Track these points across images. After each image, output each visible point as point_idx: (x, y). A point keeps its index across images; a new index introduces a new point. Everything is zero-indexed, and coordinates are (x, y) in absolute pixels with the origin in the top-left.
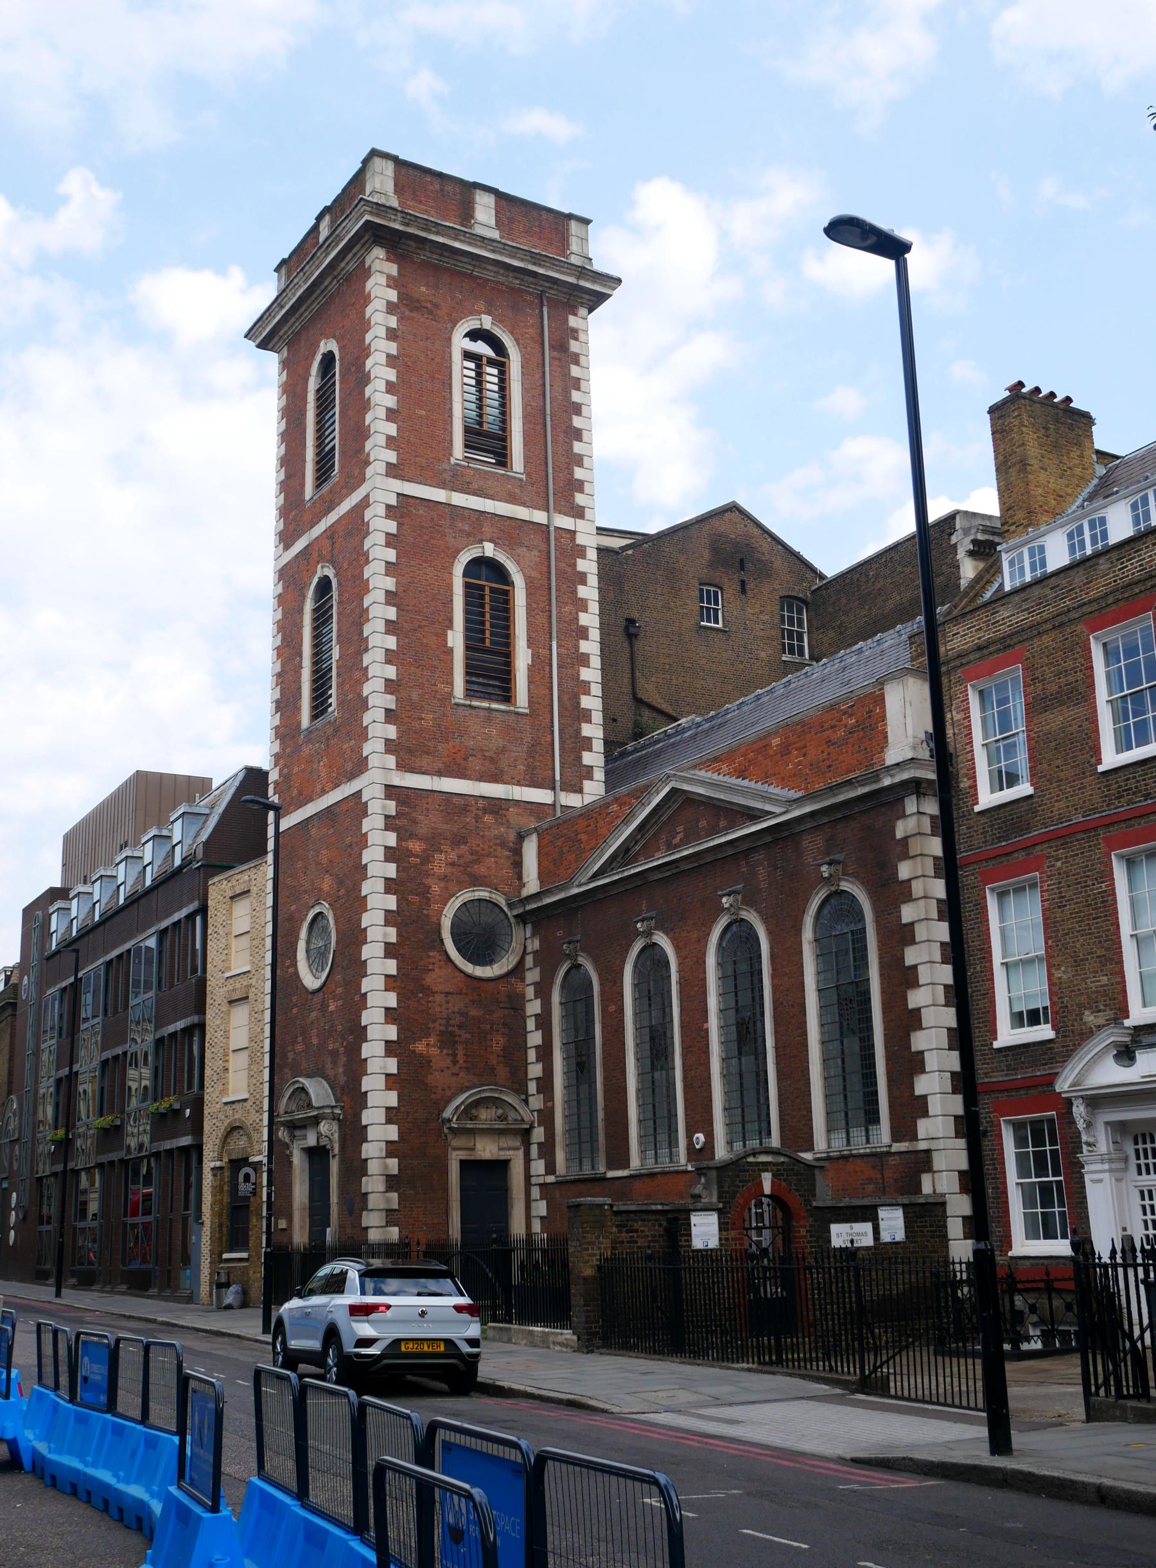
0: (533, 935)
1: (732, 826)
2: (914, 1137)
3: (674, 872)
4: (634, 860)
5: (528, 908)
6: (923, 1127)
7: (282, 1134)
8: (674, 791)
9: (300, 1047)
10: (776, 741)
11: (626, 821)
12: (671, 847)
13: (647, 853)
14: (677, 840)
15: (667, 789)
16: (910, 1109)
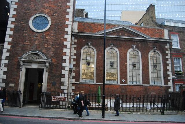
0: (75, 39)
1: (133, 36)
2: (168, 84)
3: (120, 39)
4: (108, 34)
5: (78, 34)
6: (169, 83)
7: (21, 63)
8: (123, 28)
9: (27, 43)
10: (143, 29)
11: (112, 29)
12: (118, 35)
13: (111, 34)
14: (120, 35)
15: (122, 27)
16: (166, 81)
